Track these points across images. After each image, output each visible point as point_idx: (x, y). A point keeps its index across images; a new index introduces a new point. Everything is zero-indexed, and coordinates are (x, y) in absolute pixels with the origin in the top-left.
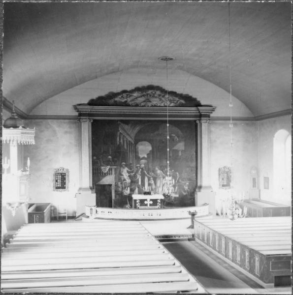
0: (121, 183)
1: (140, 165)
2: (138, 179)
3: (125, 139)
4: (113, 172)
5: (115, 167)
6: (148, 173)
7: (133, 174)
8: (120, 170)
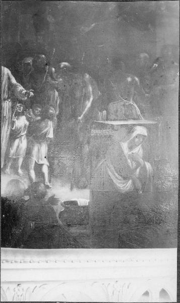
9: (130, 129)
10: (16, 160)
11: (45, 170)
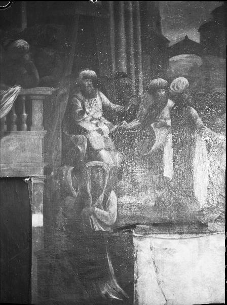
0: (78, 171)
1: (170, 81)
2: (160, 151)
4: (38, 117)
5: (49, 91)
7: (135, 123)
8: (71, 107)
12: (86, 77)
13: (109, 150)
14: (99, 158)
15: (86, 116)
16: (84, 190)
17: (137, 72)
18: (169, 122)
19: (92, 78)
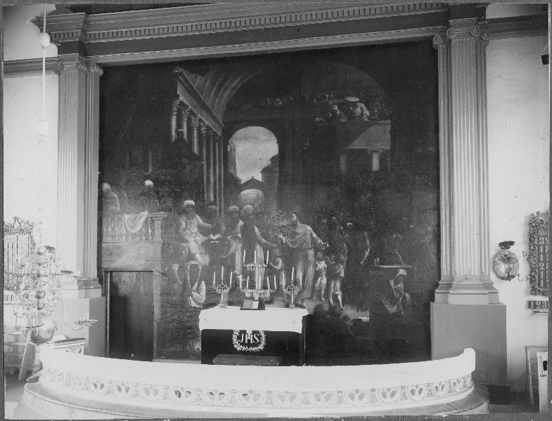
1: (241, 208)
2: (234, 255)
3: (195, 123)
6: (264, 235)
7: (218, 236)
9: (396, 270)
10: (320, 291)
11: (340, 298)
12: (189, 206)
13: (201, 253)
14: (194, 259)
15: (187, 231)
16: (185, 280)
17: (220, 200)
18: (240, 235)
19: (191, 206)
